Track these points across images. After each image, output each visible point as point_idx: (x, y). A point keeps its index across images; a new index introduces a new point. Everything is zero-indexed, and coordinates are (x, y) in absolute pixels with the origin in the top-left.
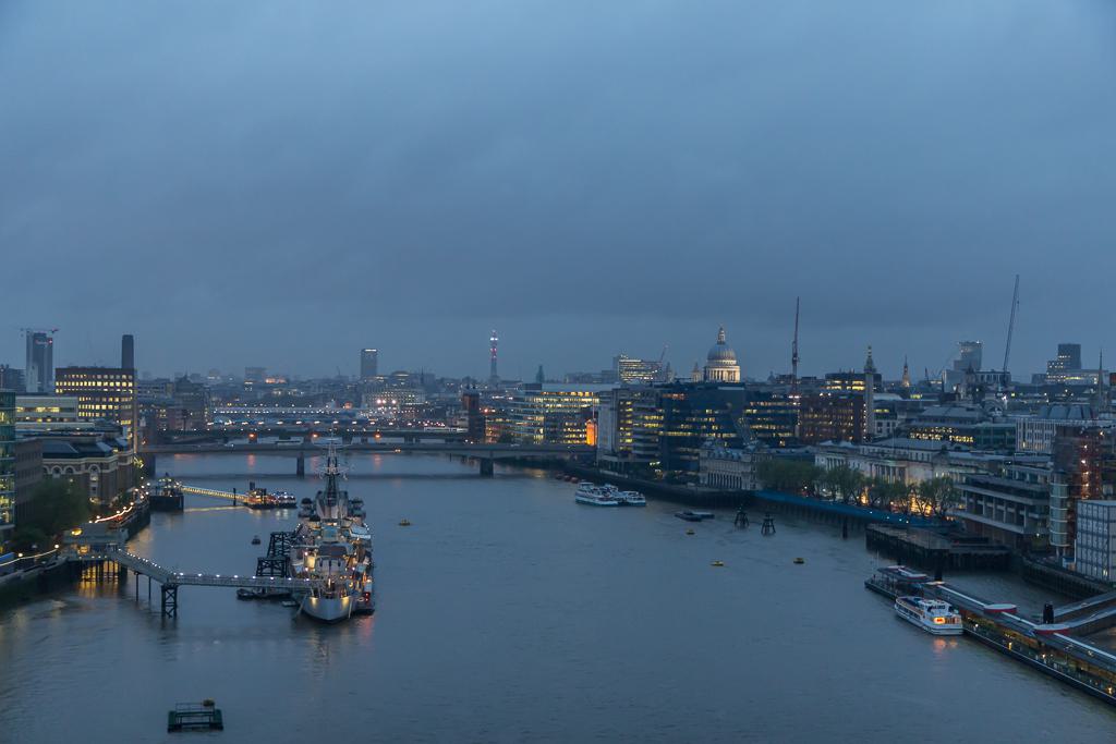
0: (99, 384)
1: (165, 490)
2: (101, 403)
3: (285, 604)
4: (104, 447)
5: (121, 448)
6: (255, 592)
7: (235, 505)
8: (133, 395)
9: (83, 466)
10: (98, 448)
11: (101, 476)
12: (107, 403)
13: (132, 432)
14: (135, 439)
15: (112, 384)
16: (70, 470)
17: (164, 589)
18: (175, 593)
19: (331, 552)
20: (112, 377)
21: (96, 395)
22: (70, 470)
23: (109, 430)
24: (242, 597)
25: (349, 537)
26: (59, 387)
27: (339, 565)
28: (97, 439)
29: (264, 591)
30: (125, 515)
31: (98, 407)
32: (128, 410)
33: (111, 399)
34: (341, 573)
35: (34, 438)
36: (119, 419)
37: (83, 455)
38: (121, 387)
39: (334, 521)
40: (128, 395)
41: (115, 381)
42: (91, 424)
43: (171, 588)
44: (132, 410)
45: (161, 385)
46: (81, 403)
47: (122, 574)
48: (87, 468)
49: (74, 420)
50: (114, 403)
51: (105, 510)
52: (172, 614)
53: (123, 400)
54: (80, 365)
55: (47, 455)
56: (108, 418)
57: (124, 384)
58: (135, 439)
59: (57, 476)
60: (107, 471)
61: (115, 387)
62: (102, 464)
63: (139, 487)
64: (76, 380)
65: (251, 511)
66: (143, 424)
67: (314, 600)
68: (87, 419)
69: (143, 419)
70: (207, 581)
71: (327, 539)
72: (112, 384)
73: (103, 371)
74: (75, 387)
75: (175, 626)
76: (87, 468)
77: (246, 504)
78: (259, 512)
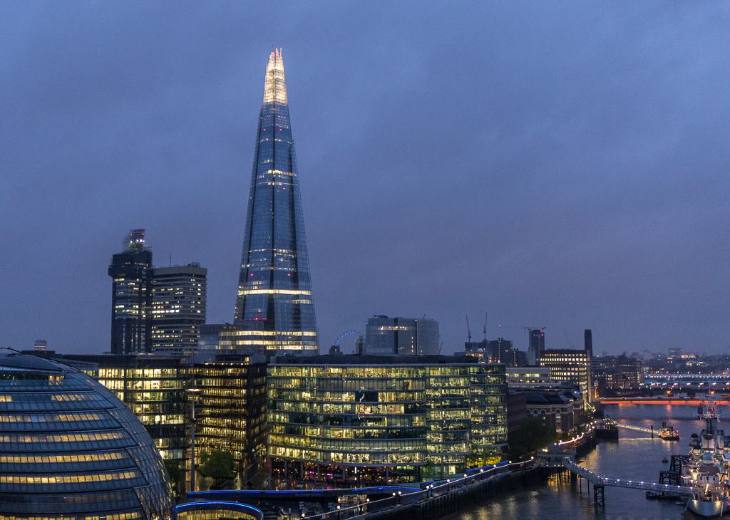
0: (566, 360)
1: (606, 426)
2: (567, 371)
3: (677, 503)
4: (563, 398)
5: (575, 399)
6: (658, 494)
7: (652, 437)
8: (587, 366)
9: (551, 410)
10: (560, 399)
11: (562, 416)
12: (571, 371)
13: (587, 389)
14: (590, 393)
15: (574, 360)
16: (543, 412)
17: (596, 488)
18: (603, 490)
19: (709, 471)
20: (573, 355)
21: (564, 366)
22: (543, 412)
23: (570, 388)
24: (651, 497)
25: (722, 461)
26: (543, 362)
27: (714, 479)
28: (559, 393)
29: (663, 493)
30: (578, 440)
31: (565, 374)
32: (584, 376)
33: (573, 369)
34: (716, 485)
35: (520, 393)
36: (578, 381)
37: (551, 403)
38: (579, 362)
39: (712, 450)
40: (584, 367)
41: (575, 357)
42: (555, 385)
43: (599, 487)
44: (587, 375)
45: (607, 360)
46: (553, 371)
47: (573, 477)
48: (553, 411)
49: (548, 382)
50: (575, 371)
51: (565, 437)
52: (601, 504)
53: (580, 369)
54: (554, 348)
55: (529, 403)
56: (571, 380)
57: (581, 360)
58: (590, 393)
59: (535, 415)
60: (567, 413)
61: (576, 362)
62: (562, 409)
63: (589, 424)
64: (552, 357)
65: (664, 442)
66: (596, 384)
67: (695, 502)
68: (556, 381)
69: (597, 381)
70: (622, 485)
71: (705, 462)
72: (574, 360)
73: (568, 352)
74: (554, 362)
75: (604, 512)
76: (553, 411)
77: (660, 437)
78: (668, 442)
